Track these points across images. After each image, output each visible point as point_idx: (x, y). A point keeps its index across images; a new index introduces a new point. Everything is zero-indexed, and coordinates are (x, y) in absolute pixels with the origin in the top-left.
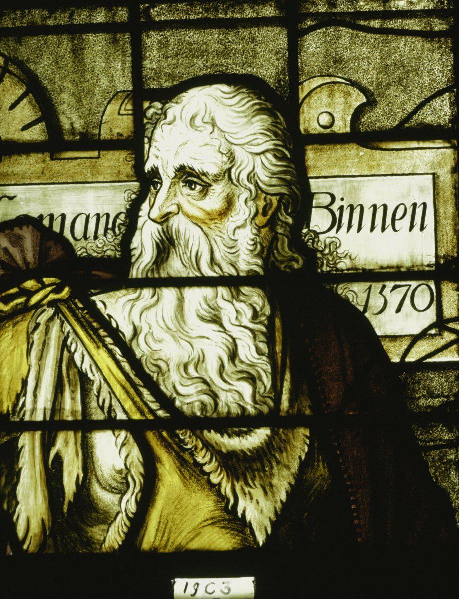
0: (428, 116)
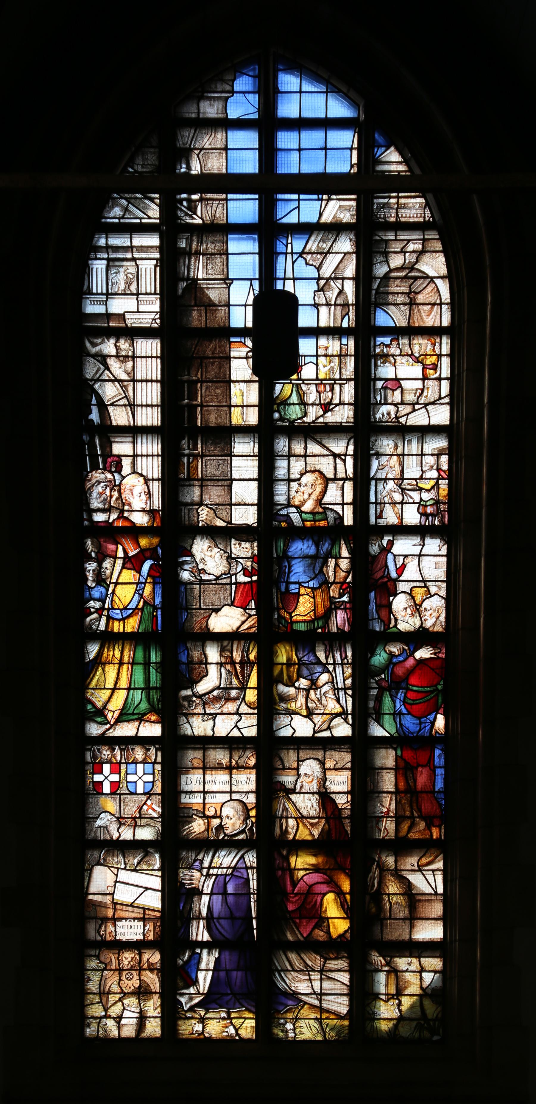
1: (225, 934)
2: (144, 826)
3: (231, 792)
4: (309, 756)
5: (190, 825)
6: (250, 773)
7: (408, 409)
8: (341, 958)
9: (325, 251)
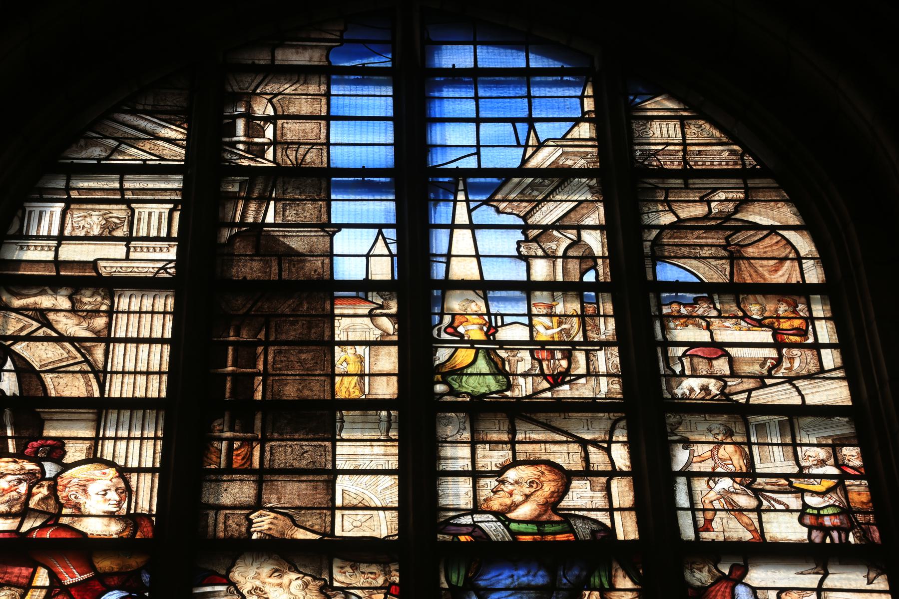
7: (749, 384)
9: (540, 198)
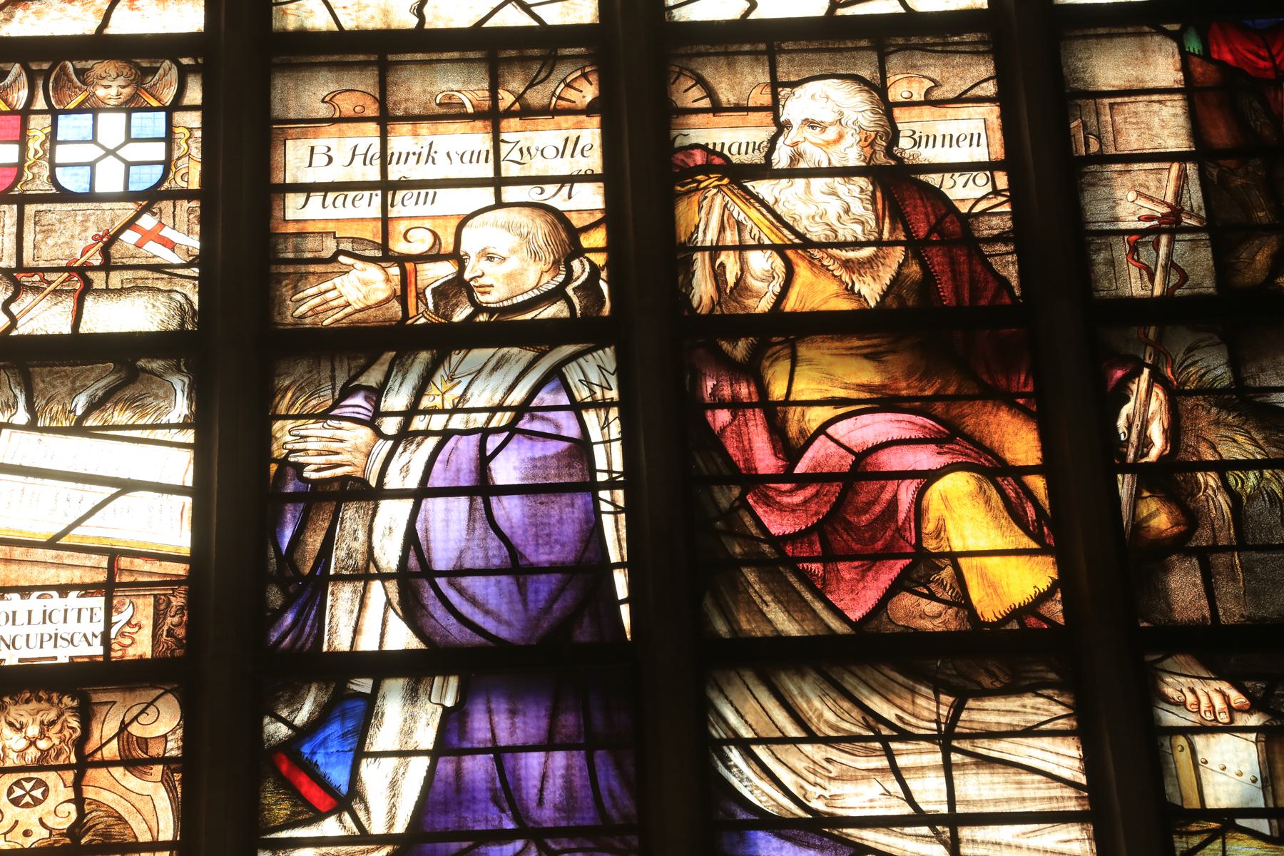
0: (978, 92)
1: (490, 625)
2: (121, 291)
3: (498, 182)
4: (817, 71)
5: (324, 287)
6: (579, 126)
8: (1034, 688)
